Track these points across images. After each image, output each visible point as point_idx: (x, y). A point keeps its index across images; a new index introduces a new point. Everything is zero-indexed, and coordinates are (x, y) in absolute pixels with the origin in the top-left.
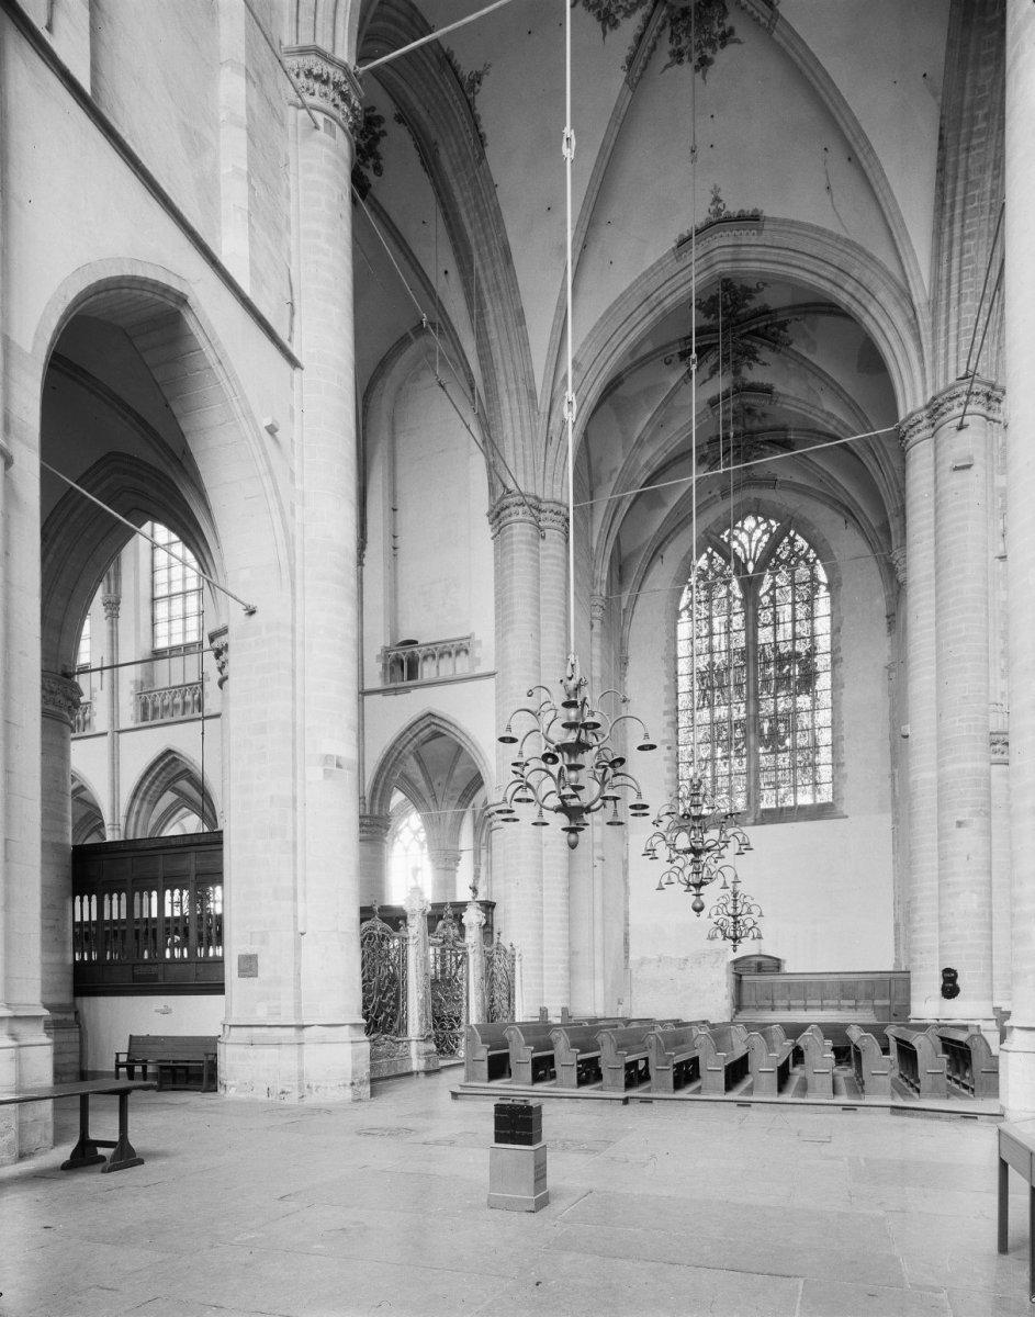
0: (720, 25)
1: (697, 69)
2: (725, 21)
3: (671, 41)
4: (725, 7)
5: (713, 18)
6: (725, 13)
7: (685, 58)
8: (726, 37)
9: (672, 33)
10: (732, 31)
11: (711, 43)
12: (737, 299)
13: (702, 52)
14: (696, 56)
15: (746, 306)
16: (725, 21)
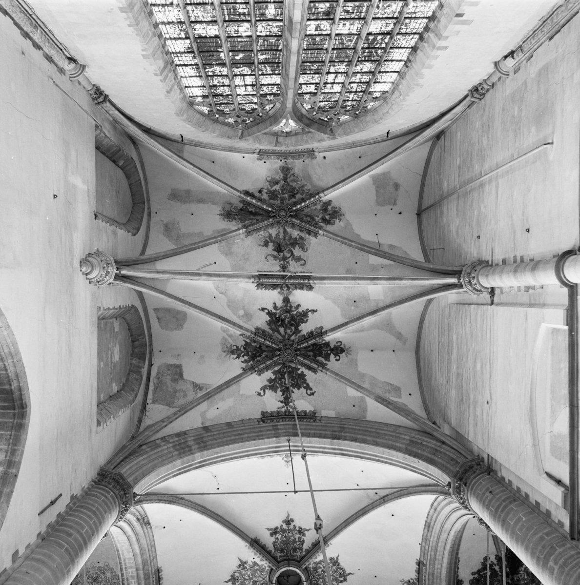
0: (277, 538)
1: (292, 520)
2: (274, 540)
3: (304, 541)
4: (274, 546)
5: (280, 542)
6: (274, 544)
7: (297, 528)
8: (274, 532)
9: (303, 544)
10: (271, 535)
11: (283, 531)
12: (281, 379)
13: (288, 527)
14: (291, 527)
15: (274, 373)
16: (274, 540)
